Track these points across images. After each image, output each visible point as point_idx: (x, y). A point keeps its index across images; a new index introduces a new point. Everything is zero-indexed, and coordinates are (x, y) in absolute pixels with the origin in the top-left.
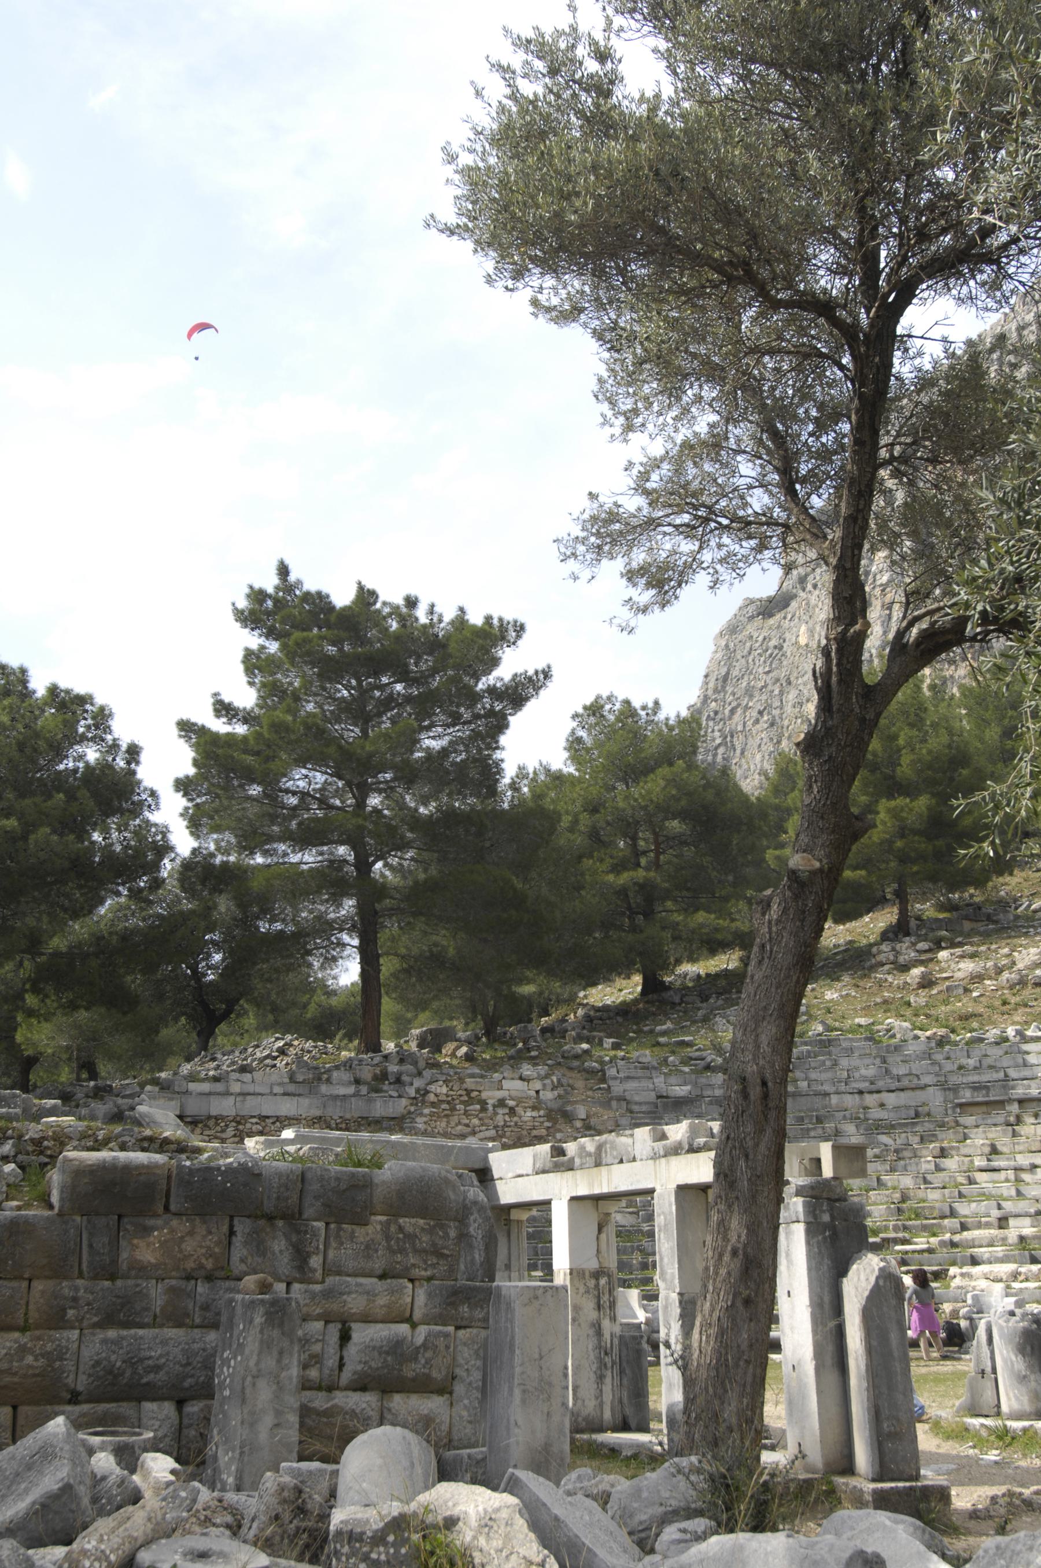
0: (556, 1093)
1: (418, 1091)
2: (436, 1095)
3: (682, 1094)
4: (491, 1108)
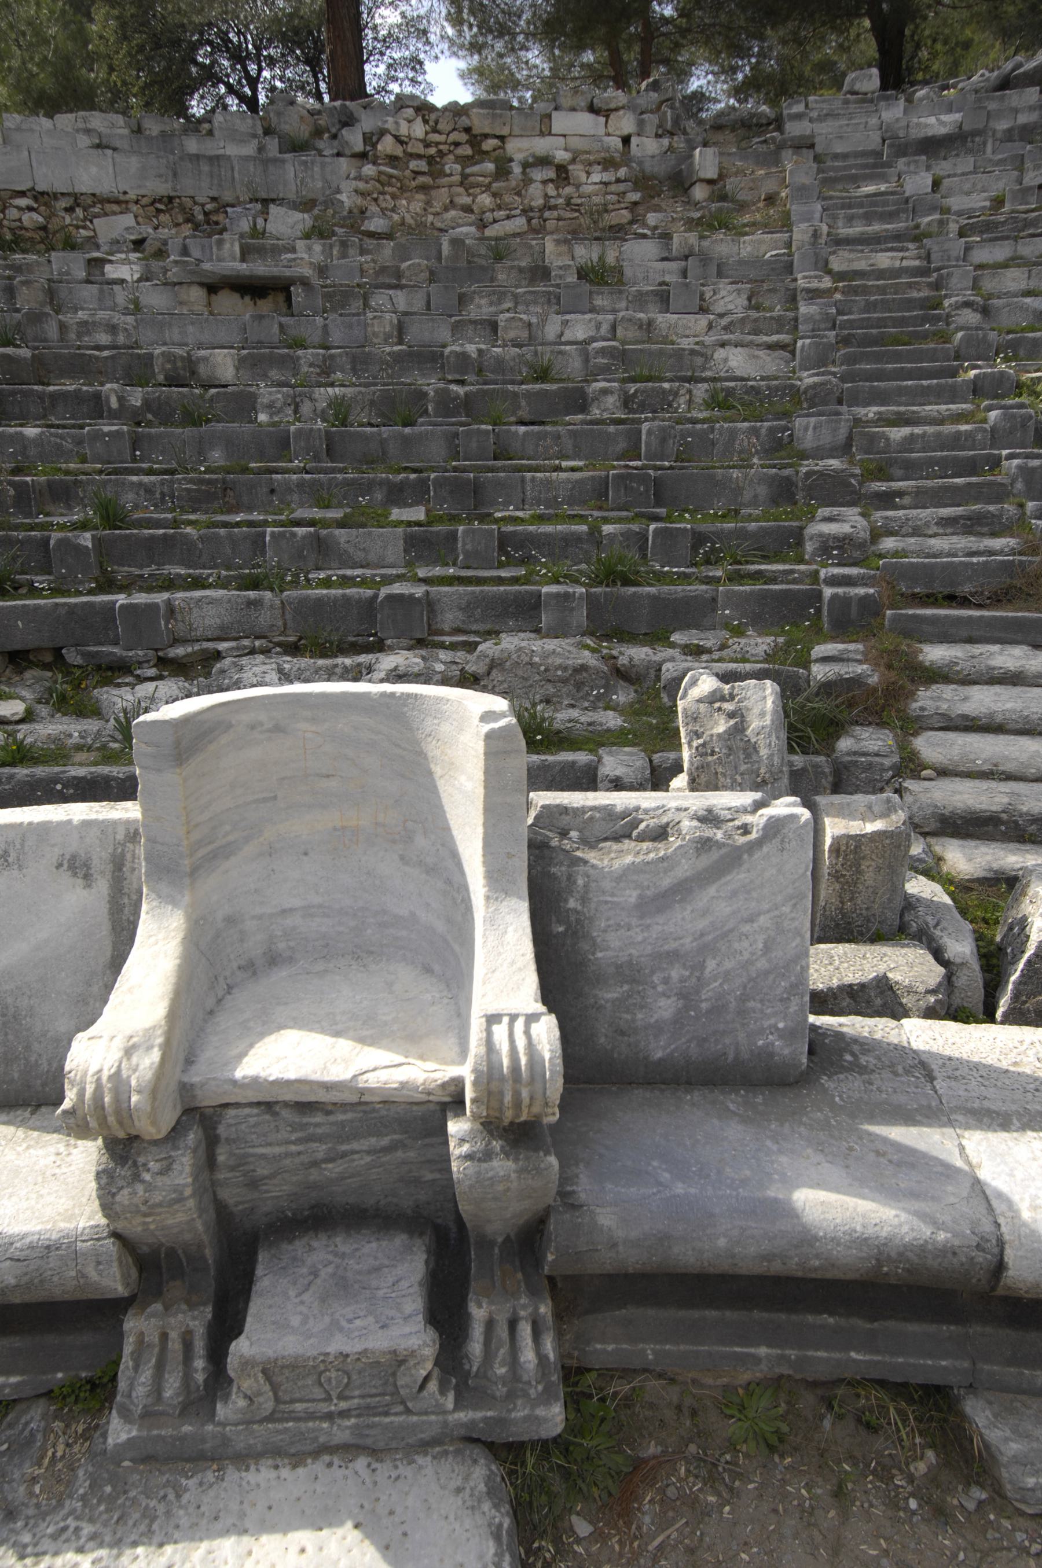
0: (666, 142)
1: (367, 138)
2: (397, 138)
3: (943, 131)
4: (517, 169)
